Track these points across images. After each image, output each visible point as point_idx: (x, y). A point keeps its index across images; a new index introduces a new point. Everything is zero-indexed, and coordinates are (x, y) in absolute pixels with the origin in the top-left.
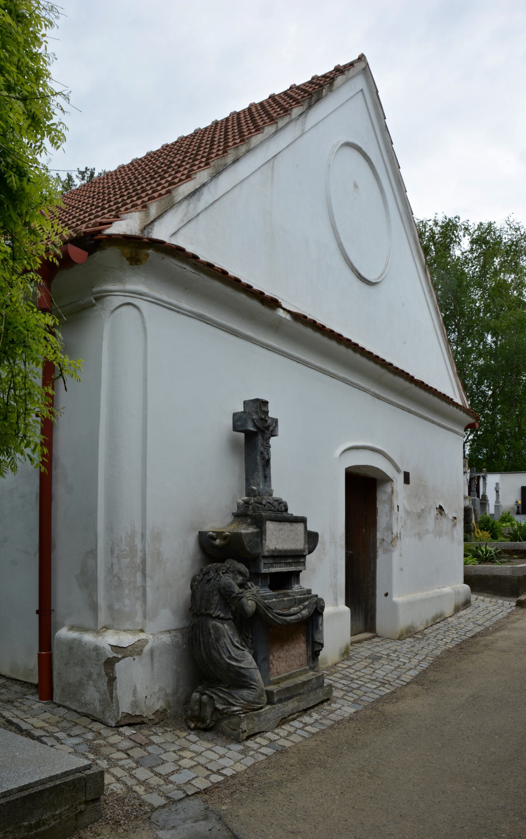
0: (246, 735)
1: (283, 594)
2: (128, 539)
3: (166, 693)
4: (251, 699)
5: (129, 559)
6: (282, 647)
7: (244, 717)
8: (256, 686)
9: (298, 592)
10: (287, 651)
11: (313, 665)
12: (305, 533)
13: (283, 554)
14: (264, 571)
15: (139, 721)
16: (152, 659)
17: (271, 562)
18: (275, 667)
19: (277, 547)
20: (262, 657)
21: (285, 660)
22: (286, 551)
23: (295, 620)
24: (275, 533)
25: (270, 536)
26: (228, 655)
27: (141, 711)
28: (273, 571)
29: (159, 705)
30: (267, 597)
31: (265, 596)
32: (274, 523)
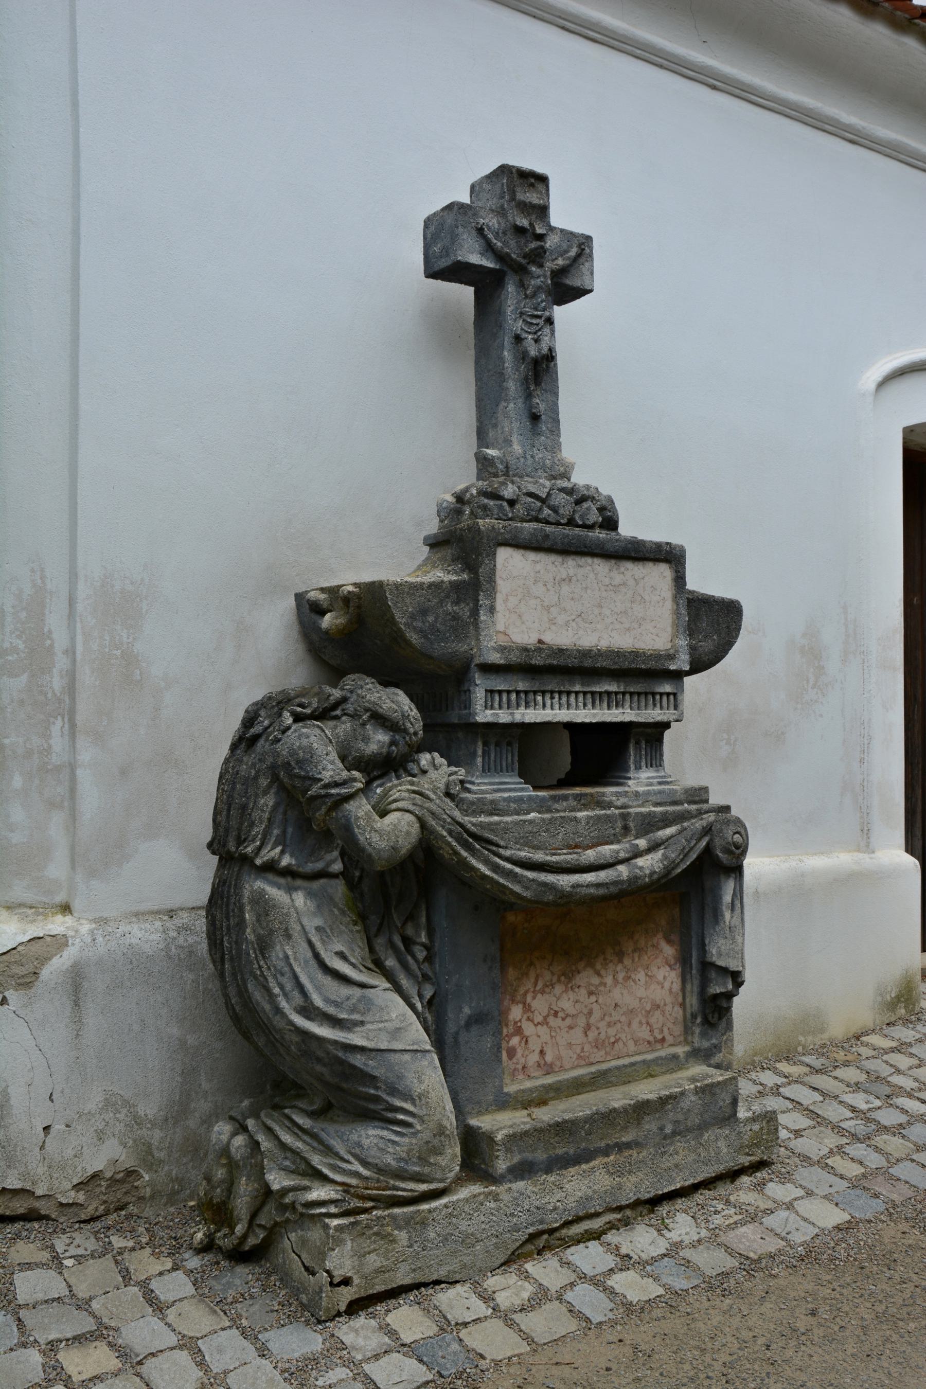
0: (346, 1295)
1: (578, 797)
2: (23, 615)
3: (135, 1117)
4: (390, 1160)
5: (24, 678)
6: (568, 977)
7: (339, 1228)
8: (412, 1114)
9: (648, 793)
10: (591, 993)
11: (706, 1044)
12: (675, 598)
13: (573, 662)
14: (484, 716)
15: (21, 1211)
16: (76, 1004)
17: (521, 686)
18: (535, 1045)
20: (467, 1010)
21: (582, 1021)
22: (586, 654)
23: (598, 885)
24: (539, 590)
25: (513, 601)
26: (298, 999)
27: (24, 1176)
28: (527, 720)
29: (105, 1156)
30: (502, 805)
31: (492, 802)
32: (532, 556)
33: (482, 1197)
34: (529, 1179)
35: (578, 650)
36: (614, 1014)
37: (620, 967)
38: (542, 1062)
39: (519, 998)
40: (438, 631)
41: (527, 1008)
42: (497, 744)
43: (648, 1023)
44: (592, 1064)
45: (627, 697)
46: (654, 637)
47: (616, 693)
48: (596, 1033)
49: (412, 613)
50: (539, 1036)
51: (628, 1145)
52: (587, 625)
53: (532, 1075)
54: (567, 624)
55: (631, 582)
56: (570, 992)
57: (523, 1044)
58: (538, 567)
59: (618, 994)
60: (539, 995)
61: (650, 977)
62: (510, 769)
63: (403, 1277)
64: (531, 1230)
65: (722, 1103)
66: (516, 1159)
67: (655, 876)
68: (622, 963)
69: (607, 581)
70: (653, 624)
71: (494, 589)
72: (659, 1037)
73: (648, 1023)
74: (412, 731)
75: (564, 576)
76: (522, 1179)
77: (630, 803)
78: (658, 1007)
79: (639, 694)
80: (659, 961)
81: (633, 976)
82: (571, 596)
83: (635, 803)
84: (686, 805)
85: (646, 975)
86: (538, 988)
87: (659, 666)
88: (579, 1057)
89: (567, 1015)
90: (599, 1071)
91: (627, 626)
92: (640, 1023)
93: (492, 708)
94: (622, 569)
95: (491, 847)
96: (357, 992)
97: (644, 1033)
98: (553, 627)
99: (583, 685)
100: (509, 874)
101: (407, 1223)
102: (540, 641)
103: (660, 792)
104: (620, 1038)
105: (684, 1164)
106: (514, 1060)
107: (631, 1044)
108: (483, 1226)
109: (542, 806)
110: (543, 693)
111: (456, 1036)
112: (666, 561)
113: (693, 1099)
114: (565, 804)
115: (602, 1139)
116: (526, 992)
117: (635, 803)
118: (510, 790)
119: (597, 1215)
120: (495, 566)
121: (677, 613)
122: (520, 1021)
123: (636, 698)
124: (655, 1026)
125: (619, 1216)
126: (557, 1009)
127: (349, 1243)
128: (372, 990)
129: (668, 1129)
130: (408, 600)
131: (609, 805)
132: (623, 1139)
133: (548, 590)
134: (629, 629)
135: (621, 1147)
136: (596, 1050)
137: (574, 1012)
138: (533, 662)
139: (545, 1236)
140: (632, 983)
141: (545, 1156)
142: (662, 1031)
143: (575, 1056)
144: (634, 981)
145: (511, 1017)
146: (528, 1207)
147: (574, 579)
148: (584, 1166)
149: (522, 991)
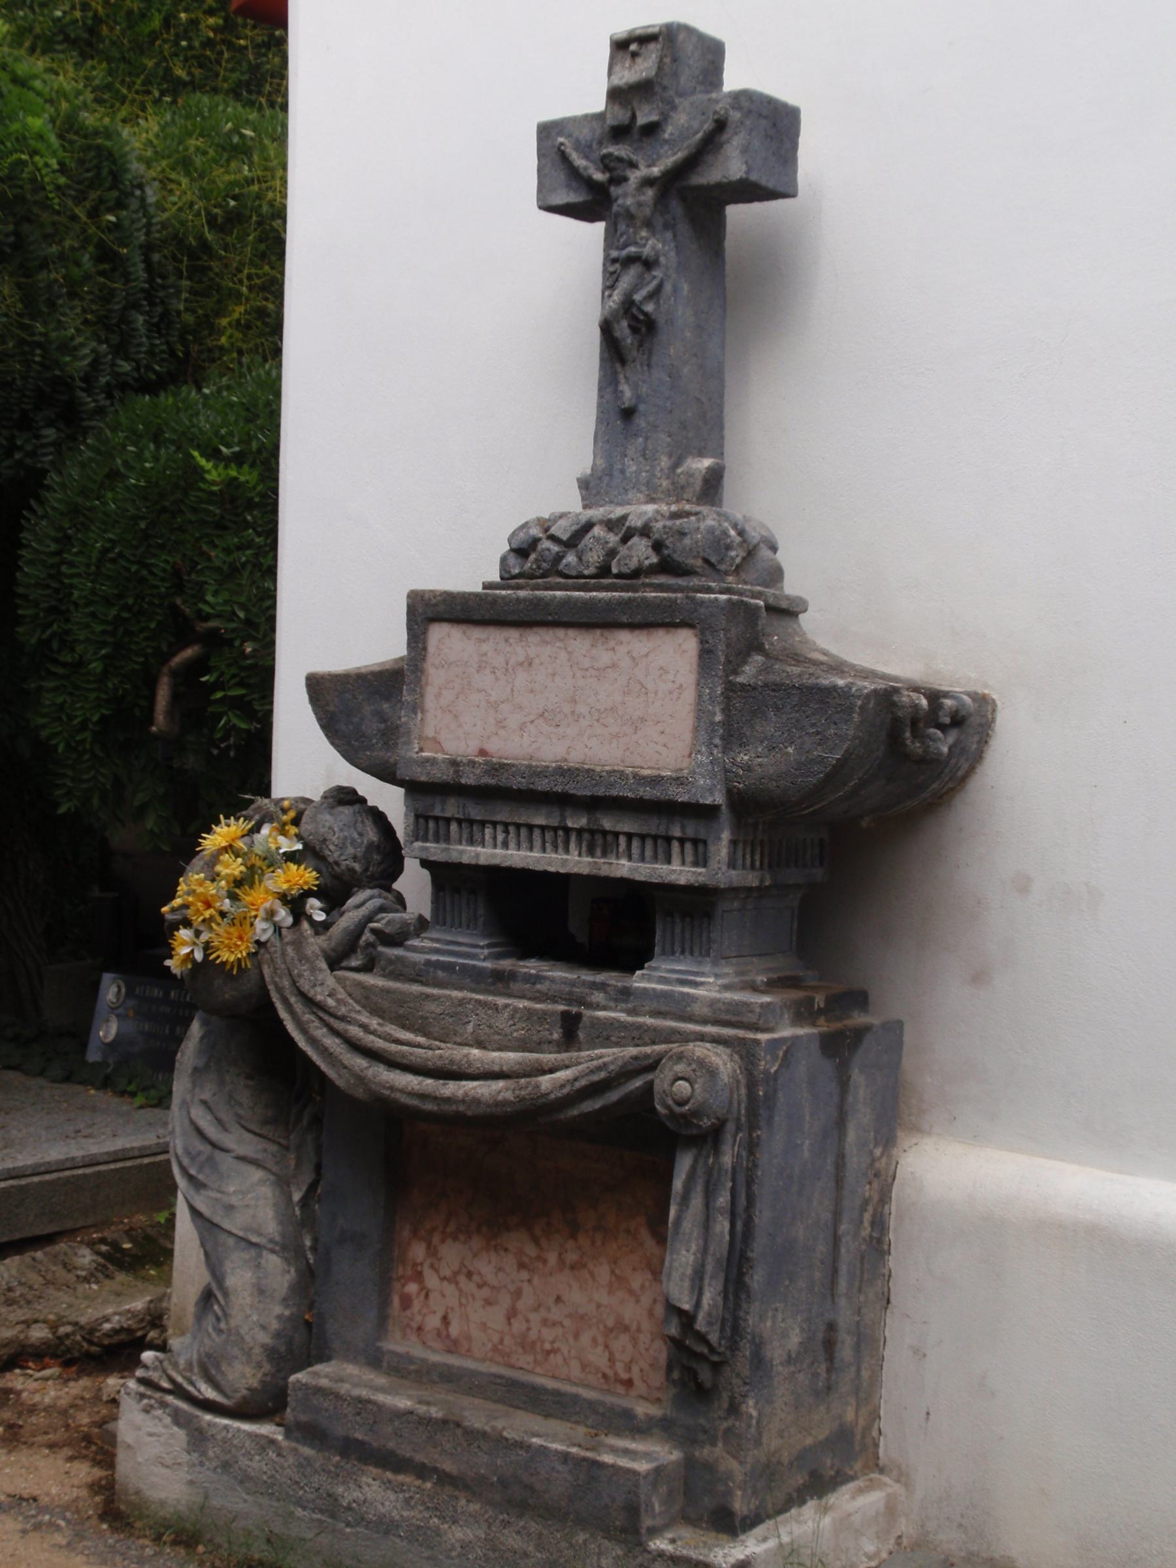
10: (522, 1266)
13: (518, 783)
23: (423, 1096)
32: (477, 633)
34: (320, 1451)
35: (530, 767)
37: (570, 1244)
38: (445, 1333)
41: (432, 1252)
43: (607, 1346)
44: (512, 1367)
46: (659, 748)
48: (524, 1326)
50: (444, 1296)
53: (430, 1343)
54: (522, 727)
57: (422, 1297)
58: (485, 647)
61: (618, 1278)
69: (587, 663)
70: (659, 727)
71: (420, 679)
72: (624, 1376)
73: (607, 1346)
78: (626, 1329)
81: (591, 1266)
85: (613, 1272)
86: (449, 1230)
88: (495, 1349)
93: (426, 840)
94: (612, 644)
95: (321, 1014)
96: (208, 1149)
97: (598, 1357)
98: (502, 732)
100: (324, 1051)
102: (483, 752)
106: (408, 1313)
107: (575, 1366)
108: (265, 1478)
110: (494, 824)
116: (434, 1229)
121: (700, 712)
122: (422, 1264)
124: (617, 1356)
126: (472, 1269)
128: (223, 1154)
133: (497, 679)
134: (616, 736)
136: (520, 1350)
138: (463, 781)
140: (588, 1276)
142: (629, 1369)
143: (490, 1346)
144: (592, 1274)
145: (411, 1254)
146: (316, 1485)
147: (537, 661)
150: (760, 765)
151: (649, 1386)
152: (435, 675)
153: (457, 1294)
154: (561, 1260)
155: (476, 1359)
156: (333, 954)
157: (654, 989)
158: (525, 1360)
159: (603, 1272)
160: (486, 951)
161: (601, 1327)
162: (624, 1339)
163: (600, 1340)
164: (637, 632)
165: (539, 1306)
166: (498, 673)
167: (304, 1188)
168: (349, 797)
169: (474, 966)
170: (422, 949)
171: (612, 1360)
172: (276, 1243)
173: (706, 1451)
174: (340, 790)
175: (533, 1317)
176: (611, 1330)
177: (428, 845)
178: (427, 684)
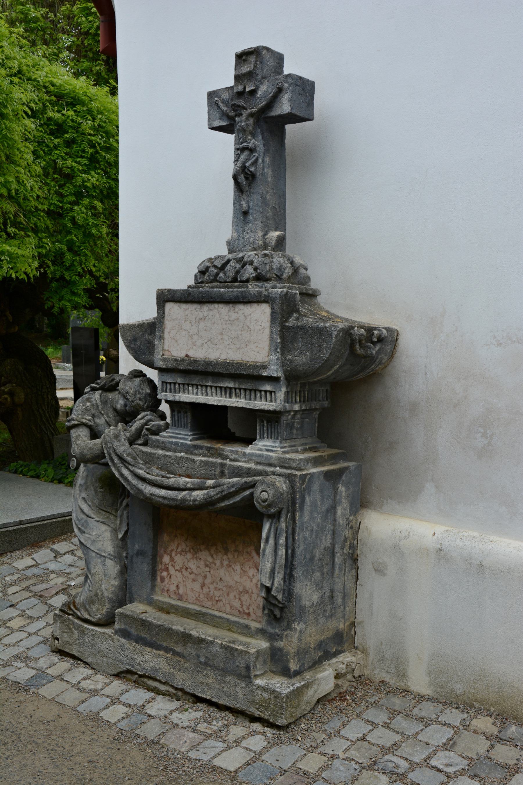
6: (195, 551)
10: (206, 566)
13: (201, 368)
17: (179, 380)
19: (191, 354)
22: (209, 363)
23: (164, 498)
25: (173, 332)
30: (168, 445)
31: (163, 442)
32: (184, 306)
33: (107, 636)
34: (128, 640)
35: (204, 361)
36: (219, 583)
37: (225, 557)
39: (168, 552)
40: (141, 349)
41: (172, 559)
42: (179, 412)
43: (240, 599)
45: (242, 391)
46: (256, 353)
47: (235, 389)
48: (208, 590)
49: (130, 340)
51: (178, 654)
52: (214, 346)
53: (172, 596)
54: (202, 345)
55: (242, 318)
56: (195, 560)
58: (187, 312)
59: (222, 572)
60: (179, 555)
61: (244, 571)
62: (185, 426)
63: (74, 651)
64: (128, 667)
65: (238, 664)
66: (123, 627)
67: (197, 503)
68: (227, 555)
69: (226, 318)
70: (256, 345)
72: (247, 611)
73: (240, 599)
74: (130, 400)
75: (201, 317)
76: (125, 638)
77: (240, 459)
78: (247, 592)
79: (250, 390)
80: (250, 563)
82: (205, 328)
83: (242, 459)
84: (278, 468)
85: (241, 569)
86: (178, 550)
87: (255, 373)
88: (197, 599)
89: (192, 573)
90: (200, 611)
91: (238, 346)
92: (235, 596)
93: (166, 392)
94: (237, 310)
96: (85, 518)
97: (236, 604)
98: (194, 347)
99: (213, 382)
100: (126, 479)
101: (78, 628)
103: (260, 456)
104: (221, 600)
105: (210, 686)
106: (163, 584)
107: (228, 606)
108: (107, 651)
109: (188, 449)
111: (132, 556)
112: (265, 302)
113: (219, 650)
114: (200, 451)
115: (164, 641)
116: (172, 550)
117: (242, 459)
118: (180, 438)
119: (165, 683)
120: (164, 313)
121: (272, 338)
122: (168, 564)
123: (248, 392)
124: (244, 603)
125: (174, 692)
127: (59, 624)
128: (90, 519)
129: (203, 659)
130: (128, 334)
131: (226, 457)
132: (175, 648)
133: (192, 325)
135: (176, 653)
136: (206, 600)
137: (197, 573)
138: (179, 367)
139: (137, 676)
140: (232, 570)
141: (136, 633)
142: (248, 609)
143: (195, 598)
144: (233, 569)
145: (164, 560)
147: (207, 318)
148: (154, 651)
149: (170, 548)
150: (296, 360)
151: (256, 616)
152: (168, 324)
153: (182, 576)
154: (222, 564)
155: (189, 603)
156: (131, 438)
157: (256, 453)
158: (208, 604)
159: (238, 568)
160: (191, 437)
161: (237, 591)
162: (246, 596)
163: (237, 596)
164: (246, 305)
165: (213, 582)
166: (193, 323)
167: (123, 533)
168: (138, 374)
169: (186, 443)
170: (165, 436)
171: (242, 605)
172: (112, 555)
173: (278, 643)
174: (135, 371)
175: (211, 586)
176: (241, 593)
177: (167, 394)
178: (165, 328)
